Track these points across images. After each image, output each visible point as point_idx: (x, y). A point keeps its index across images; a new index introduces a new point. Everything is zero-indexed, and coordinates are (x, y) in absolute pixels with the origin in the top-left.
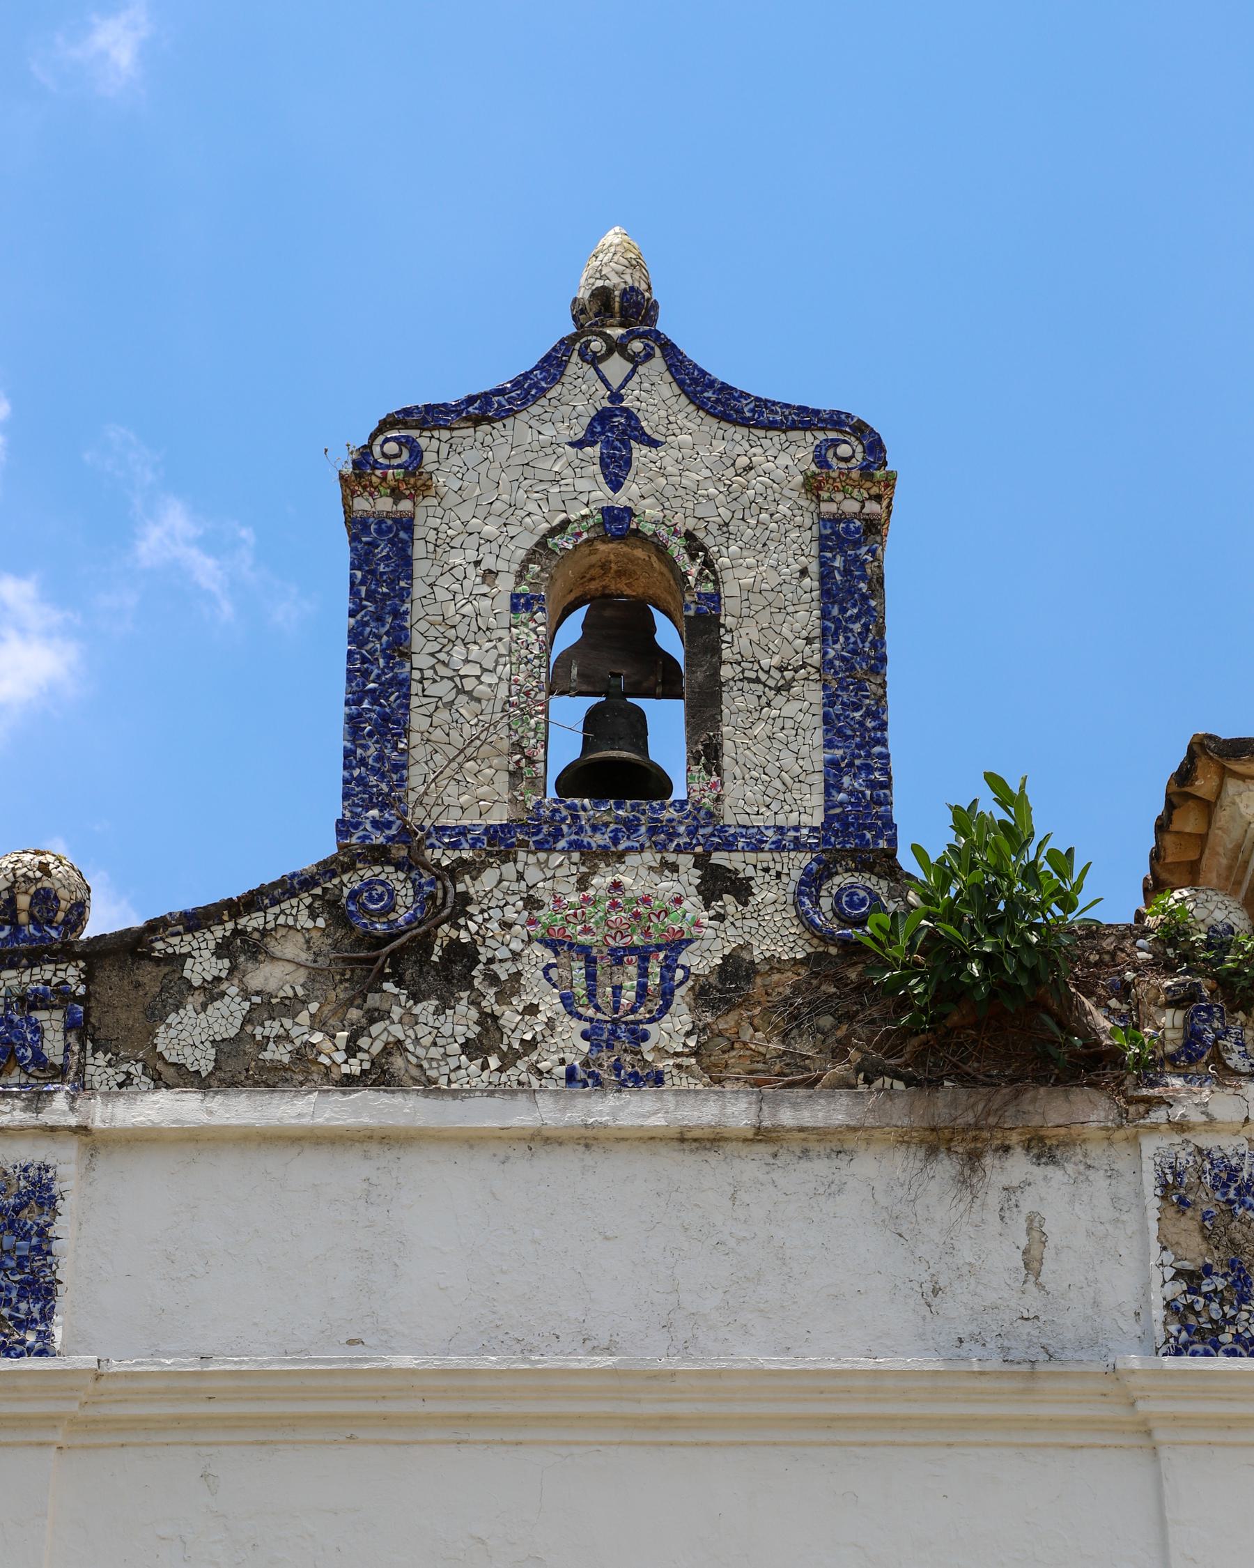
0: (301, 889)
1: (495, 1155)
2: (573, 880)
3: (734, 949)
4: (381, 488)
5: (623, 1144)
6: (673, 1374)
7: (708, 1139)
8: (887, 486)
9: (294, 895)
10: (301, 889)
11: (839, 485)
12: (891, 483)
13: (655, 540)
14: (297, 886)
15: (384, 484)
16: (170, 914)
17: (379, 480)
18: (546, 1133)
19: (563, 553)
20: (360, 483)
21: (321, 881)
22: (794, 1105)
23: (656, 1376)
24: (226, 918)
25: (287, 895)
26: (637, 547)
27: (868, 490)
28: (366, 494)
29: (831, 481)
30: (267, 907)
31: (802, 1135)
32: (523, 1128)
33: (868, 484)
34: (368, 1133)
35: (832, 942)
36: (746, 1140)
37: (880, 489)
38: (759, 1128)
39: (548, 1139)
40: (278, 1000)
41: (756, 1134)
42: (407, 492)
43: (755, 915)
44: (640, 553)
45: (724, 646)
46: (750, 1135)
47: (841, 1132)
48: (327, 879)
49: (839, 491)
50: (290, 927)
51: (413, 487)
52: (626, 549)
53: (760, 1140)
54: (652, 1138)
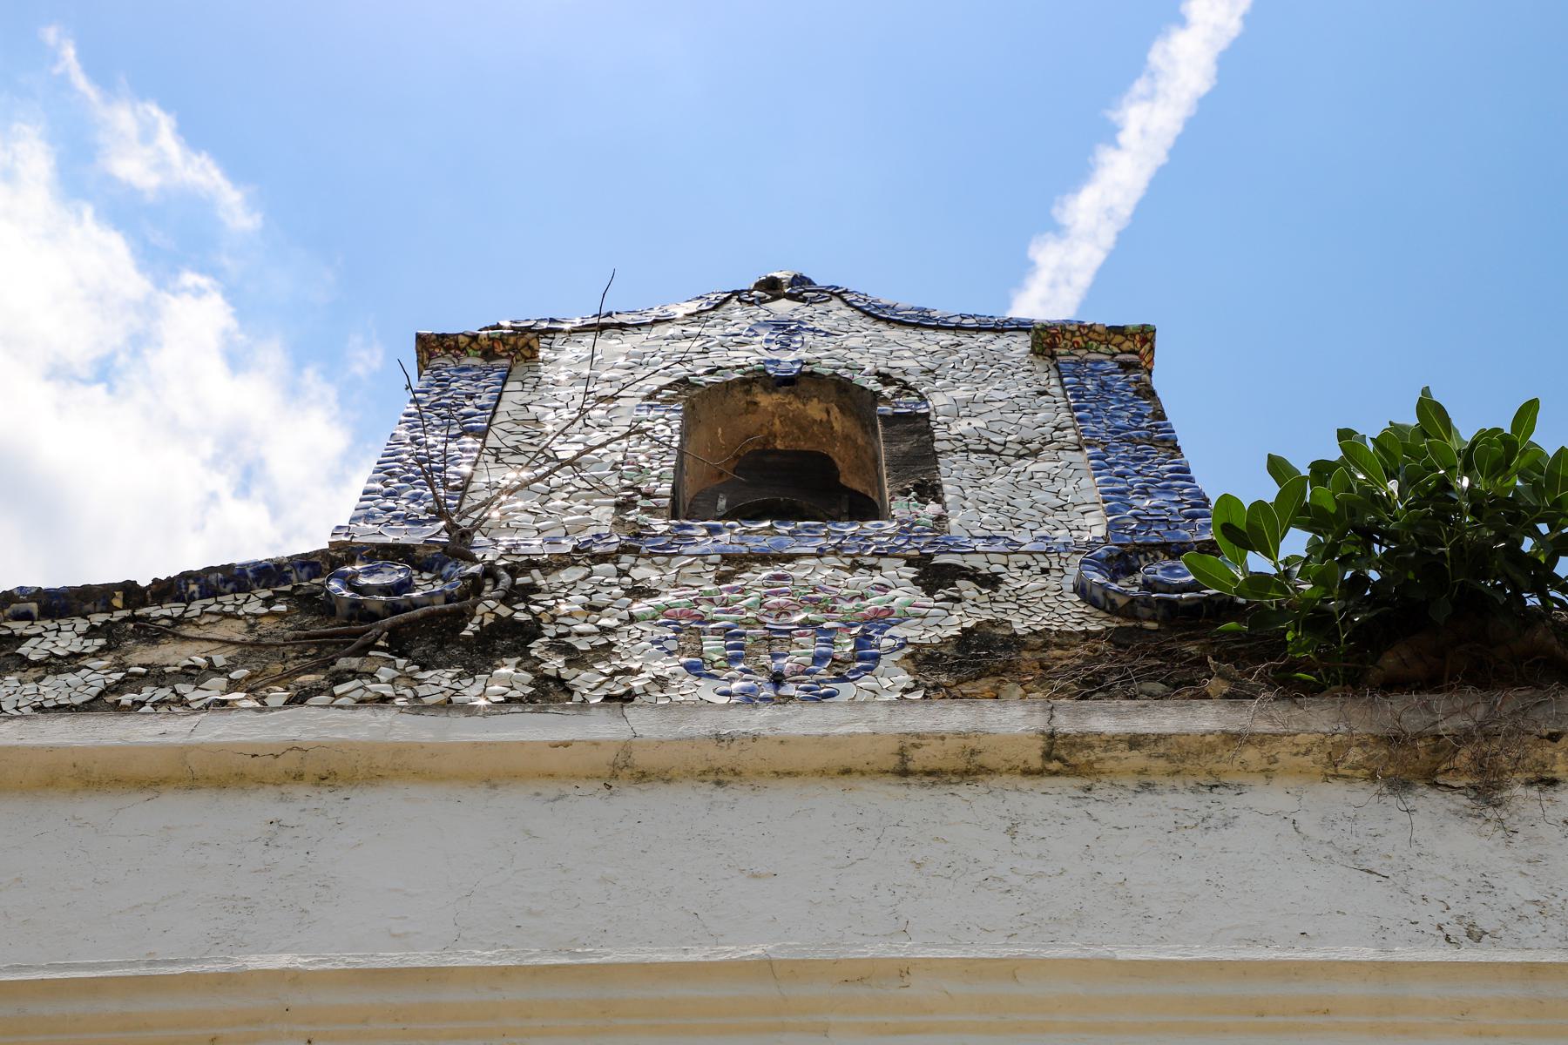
0: (257, 580)
1: (538, 794)
2: (712, 576)
3: (978, 624)
4: (470, 351)
5: (786, 781)
6: (904, 970)
7: (954, 773)
8: (1144, 341)
9: (241, 588)
10: (257, 580)
11: (1079, 339)
12: (1149, 336)
13: (836, 378)
14: (251, 575)
15: (474, 345)
16: (21, 588)
17: (467, 340)
18: (641, 759)
19: (709, 386)
20: (442, 345)
21: (293, 576)
22: (1118, 714)
23: (861, 974)
24: (117, 602)
25: (230, 586)
26: (809, 399)
27: (1118, 346)
28: (449, 355)
29: (1068, 335)
30: (192, 599)
31: (1137, 759)
32: (596, 744)
33: (1119, 339)
34: (290, 762)
35: (1147, 612)
36: (1027, 772)
37: (1135, 345)
38: (1052, 735)
39: (643, 774)
40: (178, 669)
41: (1048, 756)
42: (505, 354)
43: (1013, 599)
44: (815, 410)
45: (935, 431)
46: (1036, 763)
47: (1212, 748)
48: (304, 575)
49: (1080, 348)
50: (227, 615)
51: (513, 350)
52: (797, 405)
53: (1056, 773)
54: (847, 772)
